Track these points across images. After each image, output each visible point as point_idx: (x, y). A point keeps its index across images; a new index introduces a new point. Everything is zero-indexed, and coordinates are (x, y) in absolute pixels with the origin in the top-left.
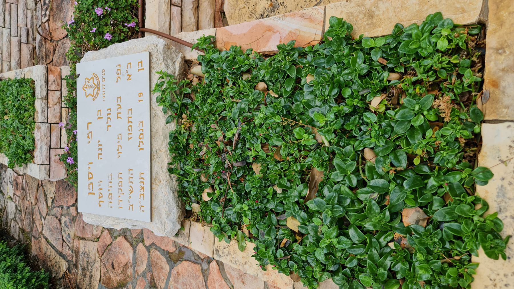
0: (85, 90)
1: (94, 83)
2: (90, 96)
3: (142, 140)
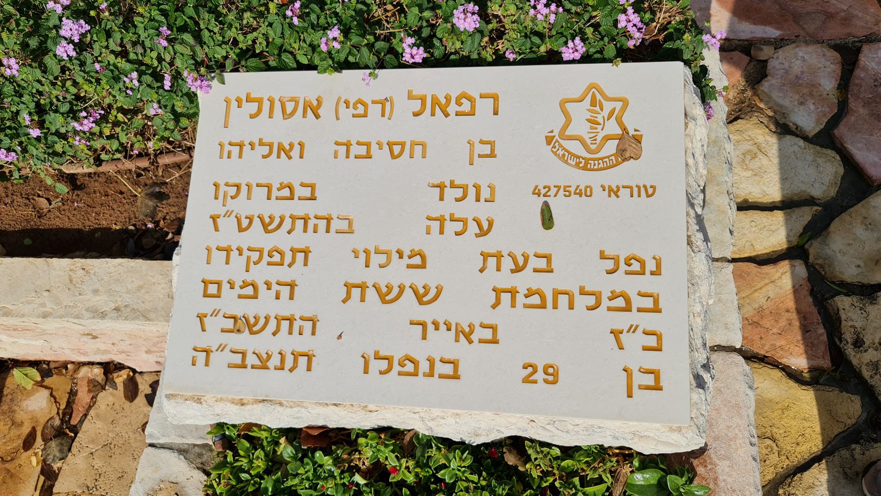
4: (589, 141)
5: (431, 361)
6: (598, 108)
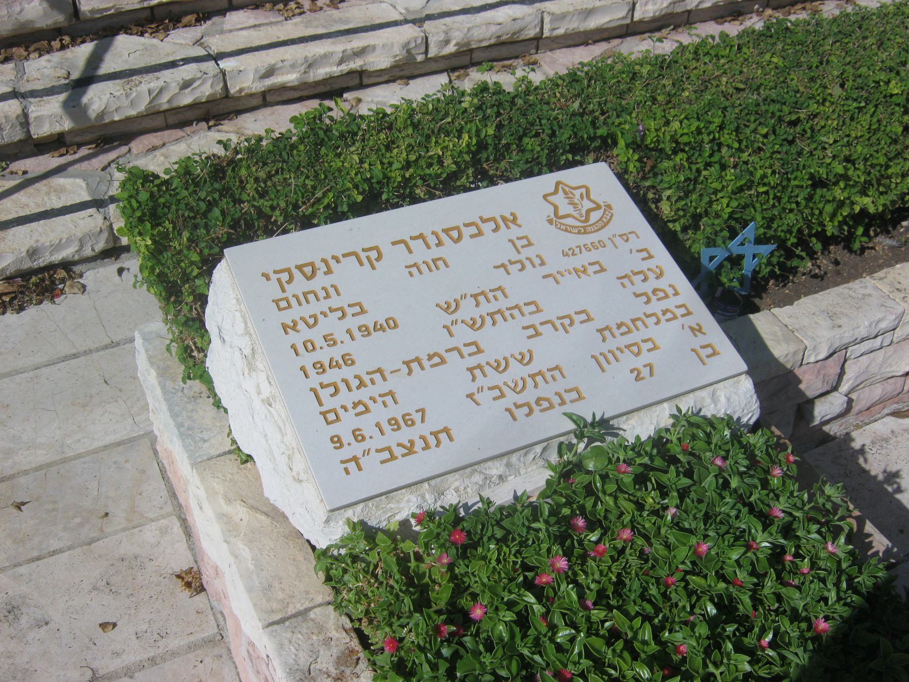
0: (556, 192)
1: (588, 212)
2: (552, 208)
3: (536, 408)
4: (578, 217)
5: (558, 394)
6: (571, 195)
